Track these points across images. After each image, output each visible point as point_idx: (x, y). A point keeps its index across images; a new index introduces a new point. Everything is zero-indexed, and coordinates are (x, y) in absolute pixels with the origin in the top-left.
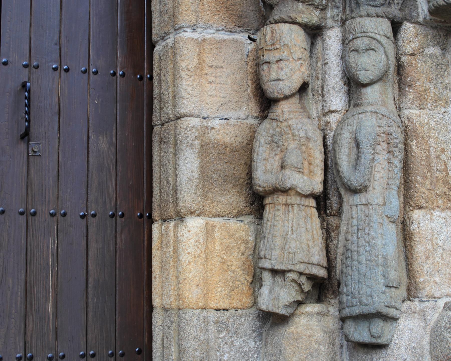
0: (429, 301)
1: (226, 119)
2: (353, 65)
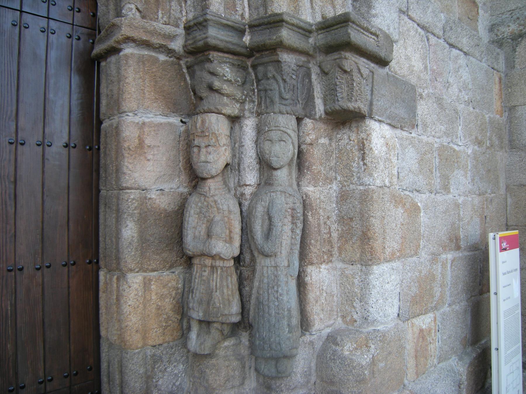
1: (161, 190)
2: (268, 152)
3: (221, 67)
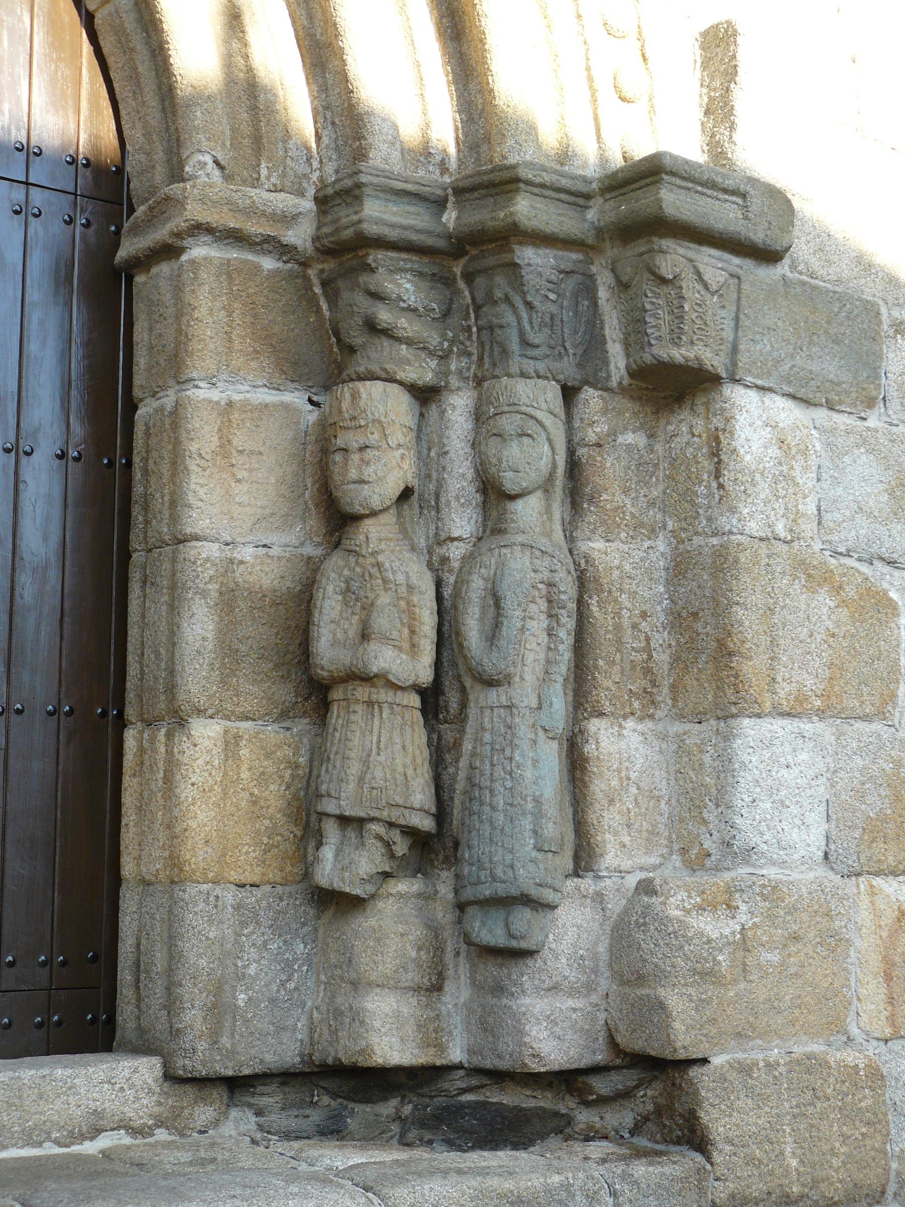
0: (610, 877)
1: (264, 546)
2: (494, 461)
3: (393, 281)
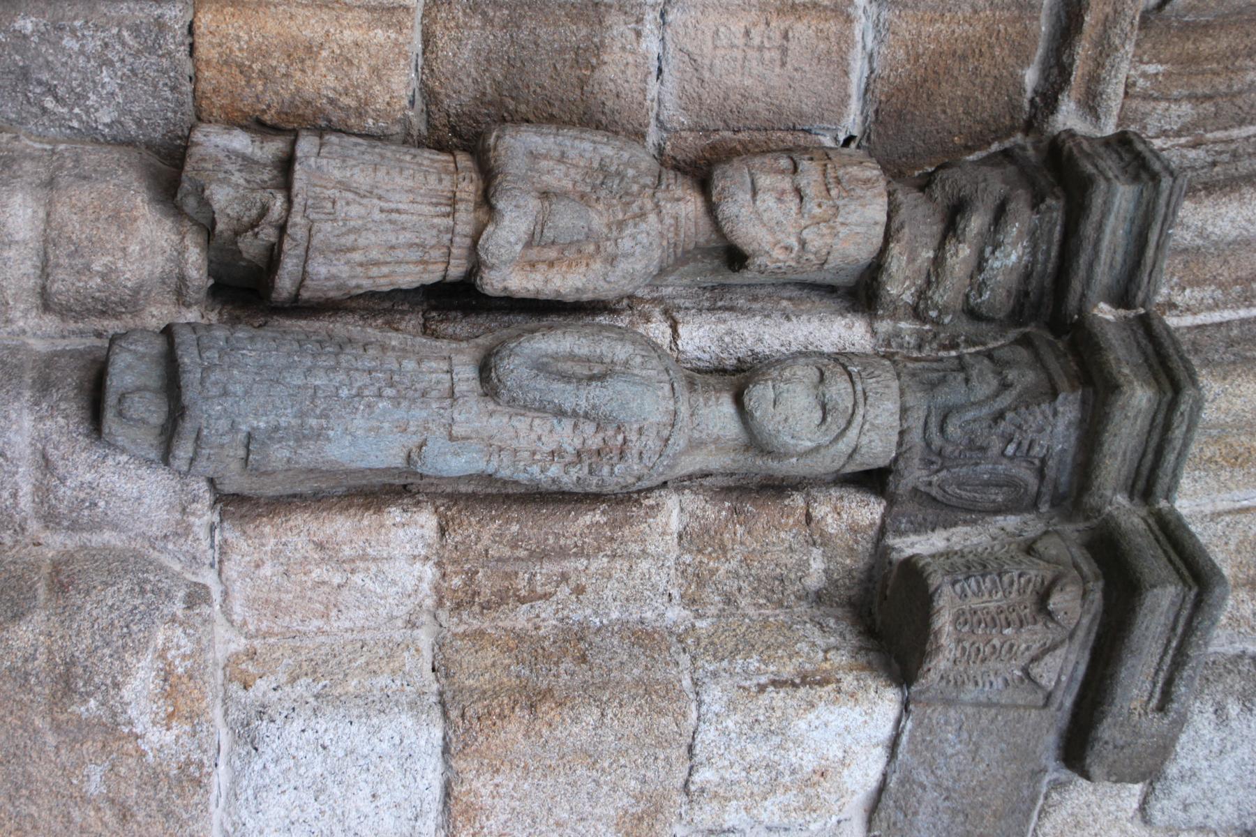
0: (212, 547)
1: (660, 70)
2: (787, 374)
3: (1020, 236)
